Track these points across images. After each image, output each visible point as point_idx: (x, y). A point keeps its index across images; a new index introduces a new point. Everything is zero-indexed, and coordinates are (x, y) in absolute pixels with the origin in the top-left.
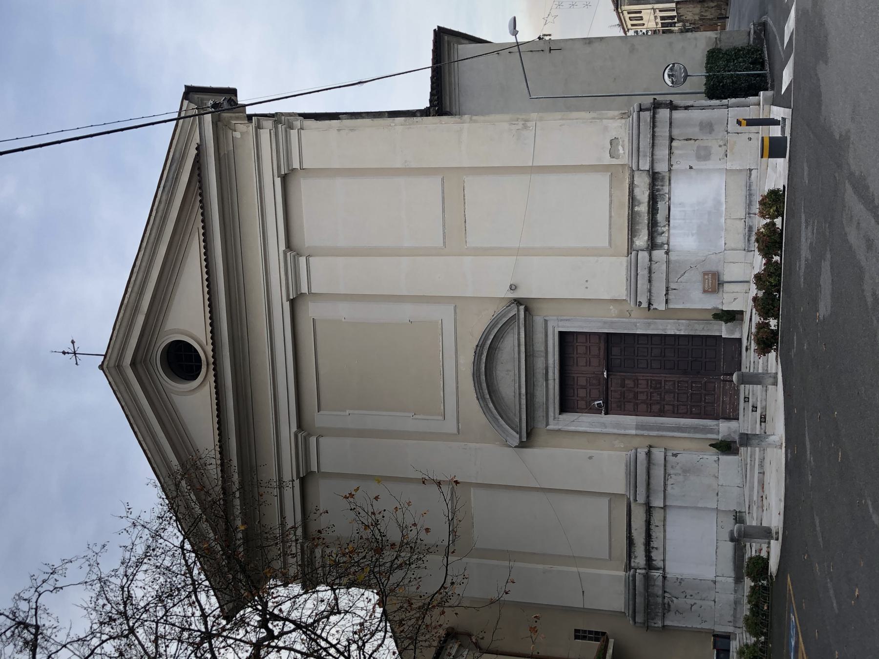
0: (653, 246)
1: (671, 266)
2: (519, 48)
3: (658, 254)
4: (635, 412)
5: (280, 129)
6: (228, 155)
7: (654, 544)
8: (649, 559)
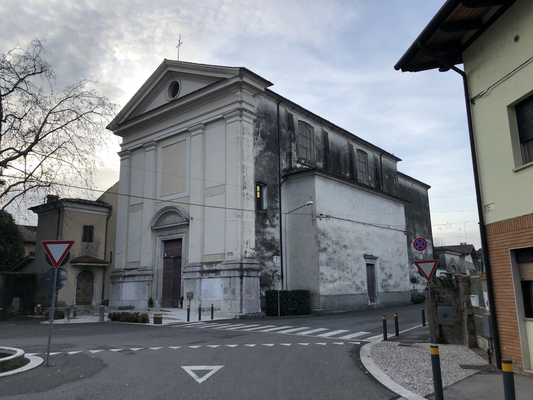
0: (202, 272)
1: (195, 280)
2: (204, 210)
3: (198, 275)
4: (164, 269)
5: (237, 112)
6: (230, 91)
7: (129, 278)
8: (125, 277)
